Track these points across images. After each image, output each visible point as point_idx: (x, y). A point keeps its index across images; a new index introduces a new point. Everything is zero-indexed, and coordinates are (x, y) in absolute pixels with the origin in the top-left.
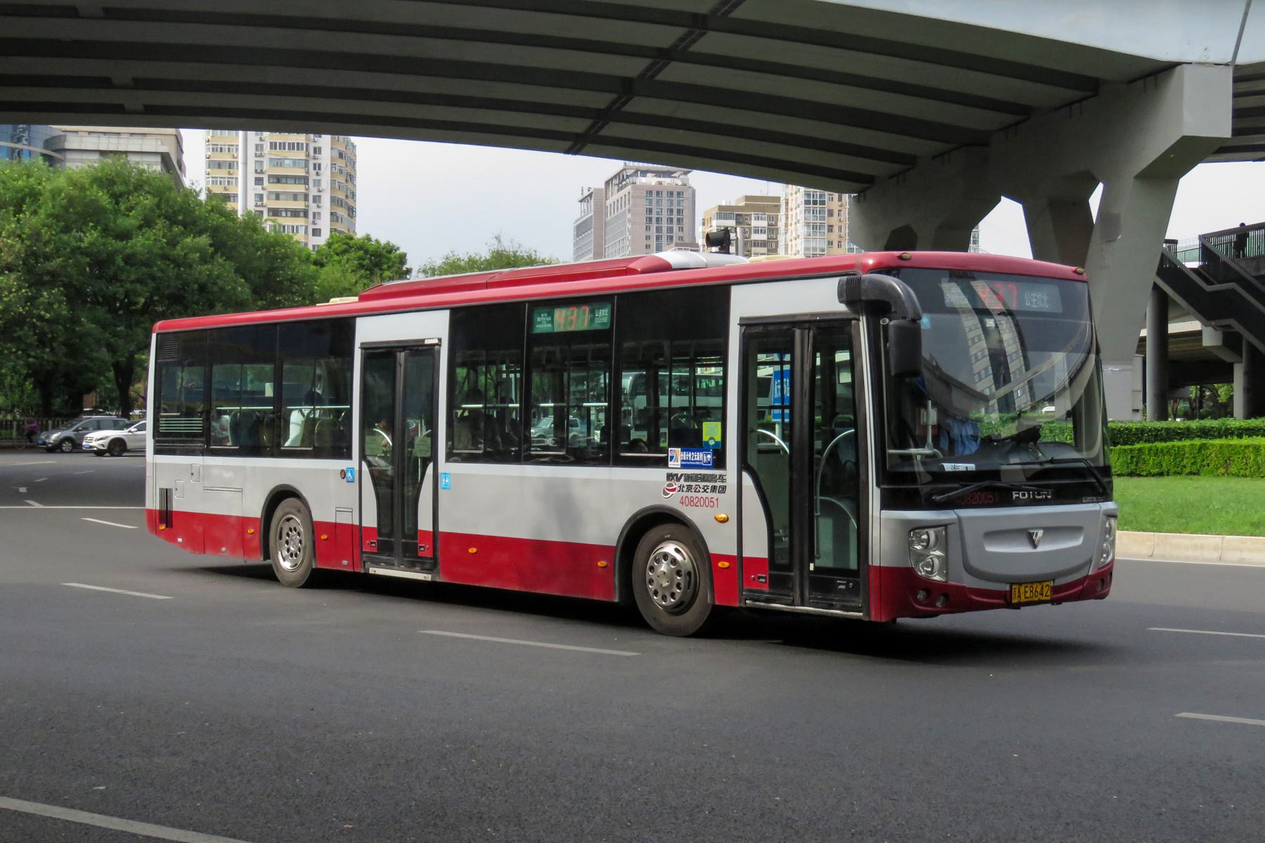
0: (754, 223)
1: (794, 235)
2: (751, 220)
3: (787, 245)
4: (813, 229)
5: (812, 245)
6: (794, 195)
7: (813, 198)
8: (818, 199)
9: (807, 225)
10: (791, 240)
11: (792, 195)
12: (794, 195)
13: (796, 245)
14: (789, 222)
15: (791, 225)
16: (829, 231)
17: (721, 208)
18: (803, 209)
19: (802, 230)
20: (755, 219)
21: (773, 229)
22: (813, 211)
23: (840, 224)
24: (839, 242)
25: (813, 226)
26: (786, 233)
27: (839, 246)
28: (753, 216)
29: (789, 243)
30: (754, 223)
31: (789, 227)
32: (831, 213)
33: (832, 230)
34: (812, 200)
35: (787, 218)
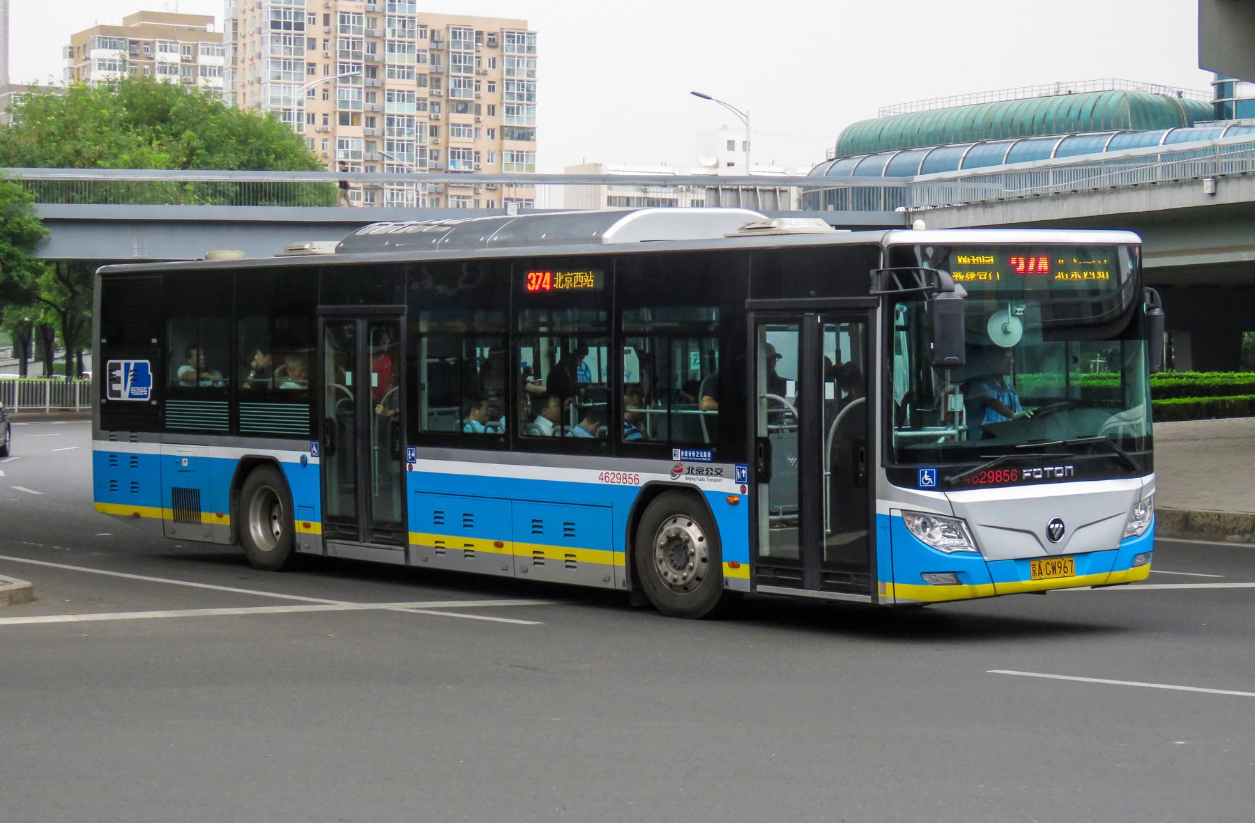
0: (159, 56)
1: (249, 76)
2: (153, 50)
3: (236, 93)
4: (285, 69)
5: (282, 94)
6: (249, 14)
7: (285, 18)
8: (293, 21)
9: (275, 61)
10: (244, 86)
11: (244, 12)
12: (248, 12)
13: (253, 91)
14: (240, 57)
15: (243, 61)
16: (308, 73)
17: (104, 30)
18: (270, 35)
19: (266, 71)
20: (161, 50)
21: (189, 68)
22: (285, 38)
23: (327, 62)
24: (326, 90)
25: (285, 63)
26: (233, 72)
27: (325, 97)
28: (157, 45)
29: (240, 91)
30: (159, 56)
31: (240, 64)
32: (312, 45)
33: (313, 70)
34: (282, 20)
35: (236, 49)
